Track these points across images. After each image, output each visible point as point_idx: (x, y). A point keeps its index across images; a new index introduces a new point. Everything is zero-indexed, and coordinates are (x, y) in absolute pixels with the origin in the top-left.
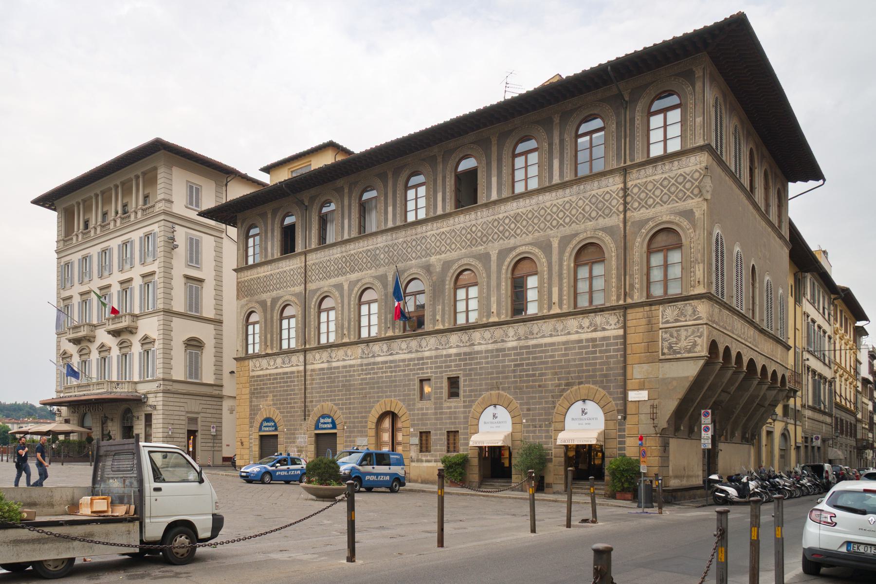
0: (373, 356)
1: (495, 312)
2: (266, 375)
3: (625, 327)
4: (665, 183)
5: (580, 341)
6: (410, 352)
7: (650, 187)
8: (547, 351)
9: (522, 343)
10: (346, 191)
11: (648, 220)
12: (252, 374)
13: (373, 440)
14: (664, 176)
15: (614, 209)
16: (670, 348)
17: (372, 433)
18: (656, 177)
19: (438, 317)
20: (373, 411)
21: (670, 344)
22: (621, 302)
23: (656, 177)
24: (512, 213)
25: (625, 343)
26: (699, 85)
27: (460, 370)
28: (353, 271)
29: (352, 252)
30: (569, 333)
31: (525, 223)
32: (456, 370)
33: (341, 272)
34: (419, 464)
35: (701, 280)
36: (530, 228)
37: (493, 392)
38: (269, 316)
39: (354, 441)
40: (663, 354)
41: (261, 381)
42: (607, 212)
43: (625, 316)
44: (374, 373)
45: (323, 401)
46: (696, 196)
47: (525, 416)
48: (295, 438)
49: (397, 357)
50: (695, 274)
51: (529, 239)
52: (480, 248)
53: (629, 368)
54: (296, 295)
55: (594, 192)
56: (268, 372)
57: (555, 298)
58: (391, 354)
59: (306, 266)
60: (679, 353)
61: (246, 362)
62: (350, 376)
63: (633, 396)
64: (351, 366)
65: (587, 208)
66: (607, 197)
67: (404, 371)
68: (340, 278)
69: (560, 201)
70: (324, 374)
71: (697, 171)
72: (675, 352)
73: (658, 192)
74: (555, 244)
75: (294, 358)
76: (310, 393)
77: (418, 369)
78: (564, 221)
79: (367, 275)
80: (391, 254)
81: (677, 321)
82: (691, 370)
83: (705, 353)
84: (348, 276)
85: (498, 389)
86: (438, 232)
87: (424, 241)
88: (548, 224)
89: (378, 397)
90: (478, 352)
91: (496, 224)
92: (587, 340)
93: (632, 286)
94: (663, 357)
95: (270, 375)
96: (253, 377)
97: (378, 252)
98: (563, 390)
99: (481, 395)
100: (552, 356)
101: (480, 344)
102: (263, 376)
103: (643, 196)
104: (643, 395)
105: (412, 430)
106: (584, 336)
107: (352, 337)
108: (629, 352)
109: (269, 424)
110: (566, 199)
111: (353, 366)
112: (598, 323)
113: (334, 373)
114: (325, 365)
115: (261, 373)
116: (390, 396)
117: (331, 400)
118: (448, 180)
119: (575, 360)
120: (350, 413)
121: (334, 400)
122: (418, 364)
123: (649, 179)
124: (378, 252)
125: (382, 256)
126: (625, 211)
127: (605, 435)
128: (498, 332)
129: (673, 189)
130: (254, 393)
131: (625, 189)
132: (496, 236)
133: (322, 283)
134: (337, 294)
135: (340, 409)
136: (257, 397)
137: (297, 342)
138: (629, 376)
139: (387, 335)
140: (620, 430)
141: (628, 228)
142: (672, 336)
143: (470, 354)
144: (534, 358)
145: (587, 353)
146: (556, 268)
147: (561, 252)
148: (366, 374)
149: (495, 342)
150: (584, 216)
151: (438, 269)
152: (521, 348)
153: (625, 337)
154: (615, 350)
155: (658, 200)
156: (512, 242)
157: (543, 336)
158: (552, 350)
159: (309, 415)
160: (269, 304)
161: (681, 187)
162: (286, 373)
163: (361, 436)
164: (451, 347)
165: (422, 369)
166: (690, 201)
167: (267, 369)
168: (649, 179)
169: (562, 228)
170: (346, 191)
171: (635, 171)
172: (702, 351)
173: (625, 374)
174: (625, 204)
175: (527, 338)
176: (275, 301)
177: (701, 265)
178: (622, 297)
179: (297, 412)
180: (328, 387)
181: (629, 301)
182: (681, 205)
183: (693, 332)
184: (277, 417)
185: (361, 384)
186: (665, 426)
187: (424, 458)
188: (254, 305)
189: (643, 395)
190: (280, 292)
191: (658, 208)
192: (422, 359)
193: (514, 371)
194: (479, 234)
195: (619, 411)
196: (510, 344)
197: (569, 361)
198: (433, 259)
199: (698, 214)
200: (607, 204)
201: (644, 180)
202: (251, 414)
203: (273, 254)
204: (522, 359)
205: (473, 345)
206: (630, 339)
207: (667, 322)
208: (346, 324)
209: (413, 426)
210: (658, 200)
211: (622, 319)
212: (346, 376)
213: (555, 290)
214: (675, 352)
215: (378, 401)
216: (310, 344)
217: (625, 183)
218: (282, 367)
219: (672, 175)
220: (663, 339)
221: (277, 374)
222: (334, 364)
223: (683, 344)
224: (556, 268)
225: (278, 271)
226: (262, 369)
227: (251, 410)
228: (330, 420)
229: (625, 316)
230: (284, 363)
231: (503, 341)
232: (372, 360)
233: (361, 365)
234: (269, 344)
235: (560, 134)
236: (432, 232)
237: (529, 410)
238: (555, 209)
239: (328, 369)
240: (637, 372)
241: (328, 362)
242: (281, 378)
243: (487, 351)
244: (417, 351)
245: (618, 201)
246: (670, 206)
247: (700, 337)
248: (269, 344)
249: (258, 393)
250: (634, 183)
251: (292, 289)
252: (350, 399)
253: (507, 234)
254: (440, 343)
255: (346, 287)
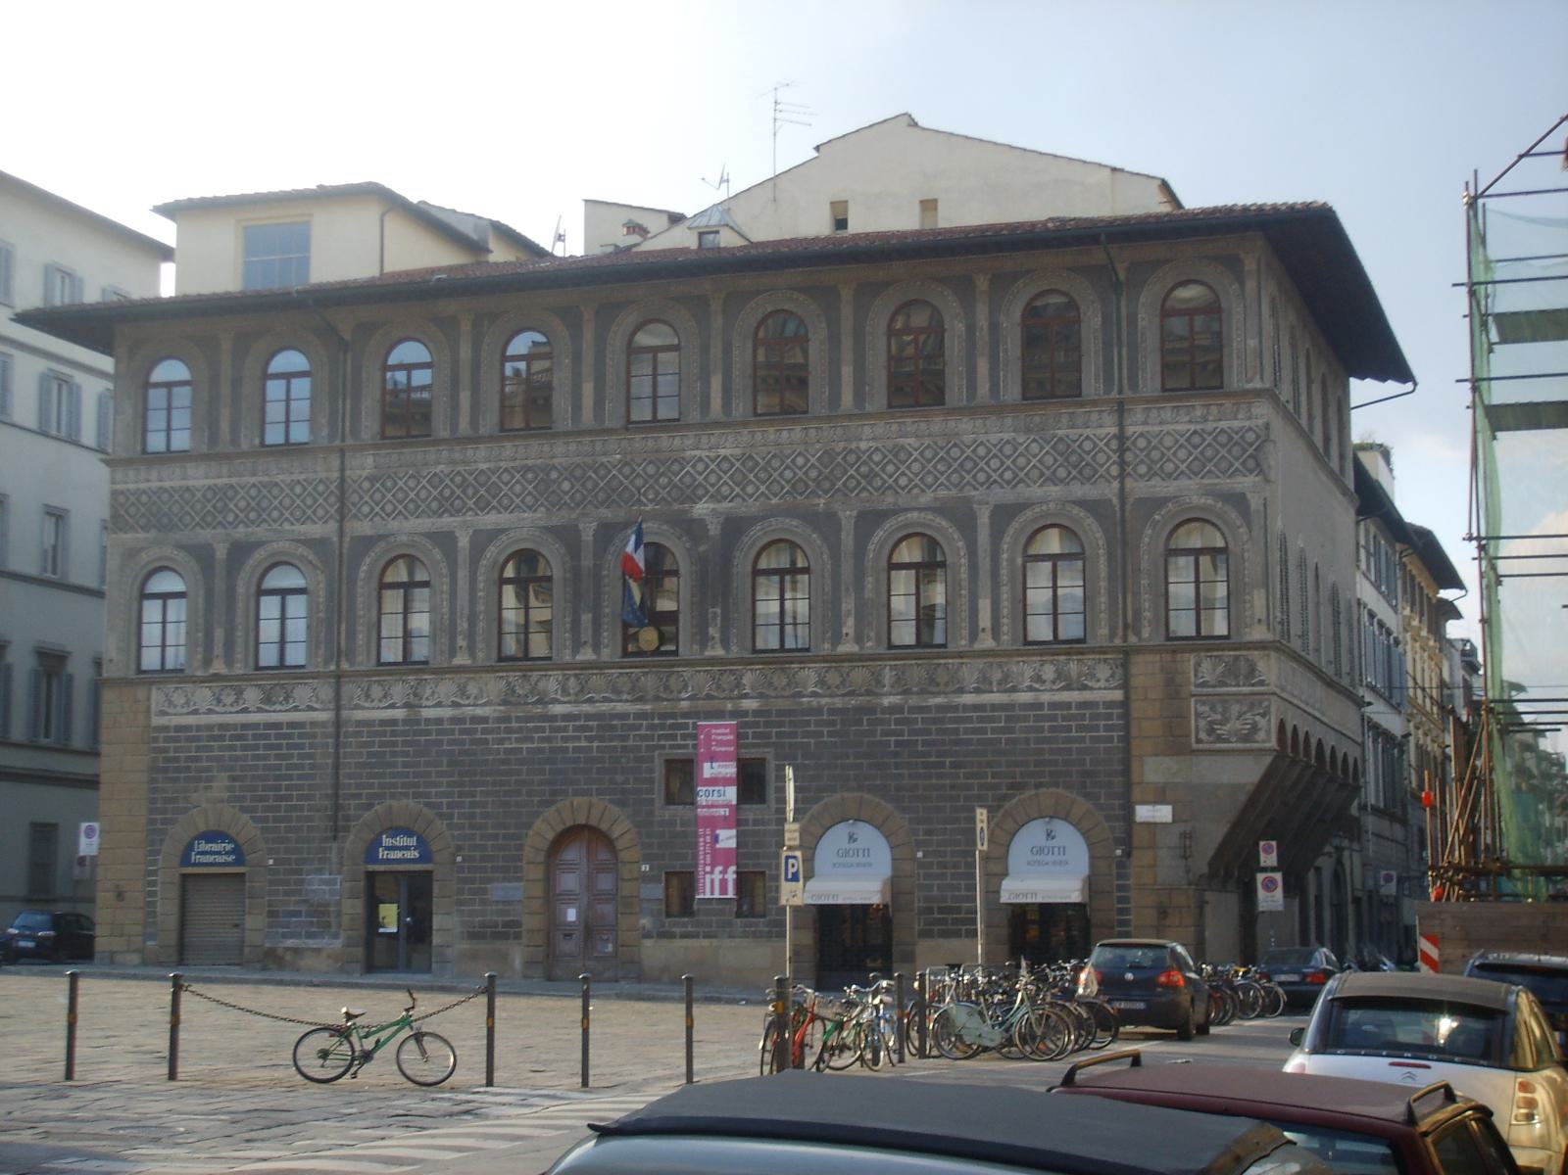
0: (539, 702)
1: (851, 632)
2: (209, 727)
3: (1125, 686)
4: (1196, 440)
5: (1039, 706)
6: (641, 699)
7: (1168, 441)
8: (969, 720)
9: (913, 701)
10: (466, 327)
11: (1165, 500)
12: (157, 721)
13: (538, 890)
14: (1193, 427)
15: (1102, 471)
16: (1211, 731)
17: (537, 873)
18: (1179, 427)
19: (711, 631)
20: (538, 825)
21: (1211, 723)
22: (1118, 642)
23: (1179, 427)
24: (889, 444)
25: (1126, 716)
26: (1250, 285)
27: (767, 745)
28: (483, 506)
29: (484, 466)
30: (1014, 689)
31: (916, 467)
32: (758, 746)
33: (447, 505)
34: (665, 942)
35: (1264, 617)
36: (930, 479)
37: (847, 795)
38: (220, 584)
39: (484, 891)
40: (1199, 741)
41: (189, 739)
42: (1087, 472)
43: (1125, 665)
44: (542, 740)
45: (393, 796)
46: (1251, 471)
47: (919, 845)
48: (302, 882)
49: (604, 707)
50: (1252, 606)
51: (926, 499)
52: (816, 501)
53: (1135, 765)
54: (318, 545)
55: (1060, 432)
56: (215, 719)
57: (985, 620)
58: (590, 701)
59: (342, 479)
60: (1227, 741)
61: (141, 693)
62: (473, 742)
63: (1143, 813)
64: (474, 719)
65: (1049, 460)
66: (1088, 445)
67: (624, 738)
68: (446, 520)
69: (994, 438)
70: (394, 733)
71: (1250, 429)
72: (1219, 739)
73: (1182, 454)
74: (984, 519)
75: (302, 693)
76: (350, 776)
77: (660, 737)
78: (1001, 476)
79: (522, 524)
80: (589, 485)
81: (1223, 684)
82: (1247, 773)
83: (1273, 743)
84: (470, 516)
85: (860, 788)
86: (712, 455)
87: (675, 467)
88: (968, 477)
89: (554, 793)
90: (810, 711)
91: (852, 458)
92: (1054, 705)
93: (1137, 614)
94: (1201, 746)
95: (221, 726)
96: (166, 728)
97: (554, 475)
98: (1005, 798)
99: (818, 800)
100: (975, 731)
101: (814, 694)
102: (199, 728)
103: (1155, 455)
104: (1164, 813)
105: (645, 868)
106: (1045, 697)
107: (480, 655)
108: (1134, 732)
109: (215, 847)
110: (1006, 436)
111: (484, 720)
112: (1074, 674)
113: (428, 733)
114: (399, 714)
115: (191, 720)
116: (587, 793)
117: (416, 796)
118: (736, 352)
119: (1027, 740)
120: (472, 827)
121: (427, 795)
122: (662, 727)
123: (1166, 428)
124: (554, 475)
125: (566, 486)
126: (1122, 476)
127: (1092, 883)
128: (859, 675)
129: (1209, 453)
130: (165, 770)
131: (1121, 437)
132: (852, 484)
133: (394, 525)
134: (437, 554)
135: (441, 815)
136: (175, 780)
137: (311, 653)
138: (1135, 778)
139: (579, 658)
140: (1120, 876)
141: (1128, 507)
142: (1213, 709)
143: (790, 713)
144: (940, 731)
145: (1052, 729)
146: (985, 564)
147: (997, 535)
148: (517, 740)
149: (851, 694)
150: (1042, 474)
151: (714, 529)
152: (912, 710)
153: (1125, 704)
154: (1107, 728)
155: (1183, 467)
156: (890, 500)
157: (961, 691)
158: (981, 720)
159: (347, 829)
160: (221, 552)
161: (1223, 452)
162: (277, 725)
163: (505, 879)
164: (746, 696)
165: (674, 737)
166: (1240, 479)
167: (210, 711)
168: (1166, 428)
169: (996, 489)
170: (466, 327)
171: (1139, 408)
172: (1268, 740)
173: (1127, 771)
174: (1122, 464)
175: (923, 692)
176: (240, 551)
177: (1263, 591)
178: (1120, 632)
179: (309, 819)
180: (405, 765)
181: (1133, 639)
182: (1225, 483)
183: (1252, 706)
184: (246, 828)
185: (503, 762)
186: (1205, 870)
187: (677, 930)
188: (168, 551)
189: (1164, 813)
190: (260, 532)
191: (1184, 483)
192: (673, 716)
193: (896, 755)
194: (813, 474)
195: (1118, 842)
196: (886, 701)
197: (1014, 741)
198: (702, 509)
199: (1255, 503)
200: (1088, 458)
201: (1157, 429)
202: (152, 822)
203: (235, 441)
204: (912, 732)
205: (800, 695)
206: (1137, 709)
207: (1204, 685)
208: (463, 625)
209: (646, 859)
210: (1183, 467)
211: (1120, 671)
212: (462, 742)
213: (985, 606)
214: (1219, 739)
215: (553, 802)
216: (352, 663)
217: (1121, 427)
218: (260, 710)
219: (1209, 426)
220: (1198, 715)
221: (245, 726)
222: (429, 713)
223: (1234, 725)
224: (985, 564)
225: (253, 480)
226: (195, 712)
227: (151, 811)
228: (413, 841)
229: (1125, 665)
230: (268, 700)
231: (869, 693)
232: (539, 710)
233: (506, 719)
234: (219, 650)
235: (991, 314)
236: (697, 453)
237: (929, 833)
238: (981, 451)
239: (406, 722)
240: (1153, 769)
241: (407, 705)
242: (255, 737)
243: (832, 711)
244: (657, 699)
245: (1109, 458)
246: (1206, 481)
247: (1263, 715)
248: (219, 650)
249: (178, 770)
250: (1140, 429)
251: (298, 527)
252: (473, 794)
253: (878, 482)
254: (719, 687)
255: (464, 542)
